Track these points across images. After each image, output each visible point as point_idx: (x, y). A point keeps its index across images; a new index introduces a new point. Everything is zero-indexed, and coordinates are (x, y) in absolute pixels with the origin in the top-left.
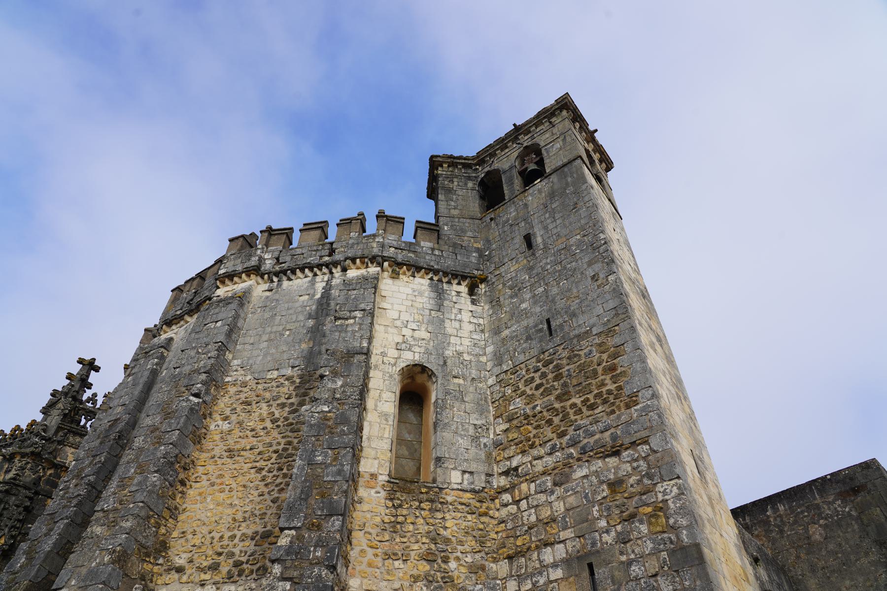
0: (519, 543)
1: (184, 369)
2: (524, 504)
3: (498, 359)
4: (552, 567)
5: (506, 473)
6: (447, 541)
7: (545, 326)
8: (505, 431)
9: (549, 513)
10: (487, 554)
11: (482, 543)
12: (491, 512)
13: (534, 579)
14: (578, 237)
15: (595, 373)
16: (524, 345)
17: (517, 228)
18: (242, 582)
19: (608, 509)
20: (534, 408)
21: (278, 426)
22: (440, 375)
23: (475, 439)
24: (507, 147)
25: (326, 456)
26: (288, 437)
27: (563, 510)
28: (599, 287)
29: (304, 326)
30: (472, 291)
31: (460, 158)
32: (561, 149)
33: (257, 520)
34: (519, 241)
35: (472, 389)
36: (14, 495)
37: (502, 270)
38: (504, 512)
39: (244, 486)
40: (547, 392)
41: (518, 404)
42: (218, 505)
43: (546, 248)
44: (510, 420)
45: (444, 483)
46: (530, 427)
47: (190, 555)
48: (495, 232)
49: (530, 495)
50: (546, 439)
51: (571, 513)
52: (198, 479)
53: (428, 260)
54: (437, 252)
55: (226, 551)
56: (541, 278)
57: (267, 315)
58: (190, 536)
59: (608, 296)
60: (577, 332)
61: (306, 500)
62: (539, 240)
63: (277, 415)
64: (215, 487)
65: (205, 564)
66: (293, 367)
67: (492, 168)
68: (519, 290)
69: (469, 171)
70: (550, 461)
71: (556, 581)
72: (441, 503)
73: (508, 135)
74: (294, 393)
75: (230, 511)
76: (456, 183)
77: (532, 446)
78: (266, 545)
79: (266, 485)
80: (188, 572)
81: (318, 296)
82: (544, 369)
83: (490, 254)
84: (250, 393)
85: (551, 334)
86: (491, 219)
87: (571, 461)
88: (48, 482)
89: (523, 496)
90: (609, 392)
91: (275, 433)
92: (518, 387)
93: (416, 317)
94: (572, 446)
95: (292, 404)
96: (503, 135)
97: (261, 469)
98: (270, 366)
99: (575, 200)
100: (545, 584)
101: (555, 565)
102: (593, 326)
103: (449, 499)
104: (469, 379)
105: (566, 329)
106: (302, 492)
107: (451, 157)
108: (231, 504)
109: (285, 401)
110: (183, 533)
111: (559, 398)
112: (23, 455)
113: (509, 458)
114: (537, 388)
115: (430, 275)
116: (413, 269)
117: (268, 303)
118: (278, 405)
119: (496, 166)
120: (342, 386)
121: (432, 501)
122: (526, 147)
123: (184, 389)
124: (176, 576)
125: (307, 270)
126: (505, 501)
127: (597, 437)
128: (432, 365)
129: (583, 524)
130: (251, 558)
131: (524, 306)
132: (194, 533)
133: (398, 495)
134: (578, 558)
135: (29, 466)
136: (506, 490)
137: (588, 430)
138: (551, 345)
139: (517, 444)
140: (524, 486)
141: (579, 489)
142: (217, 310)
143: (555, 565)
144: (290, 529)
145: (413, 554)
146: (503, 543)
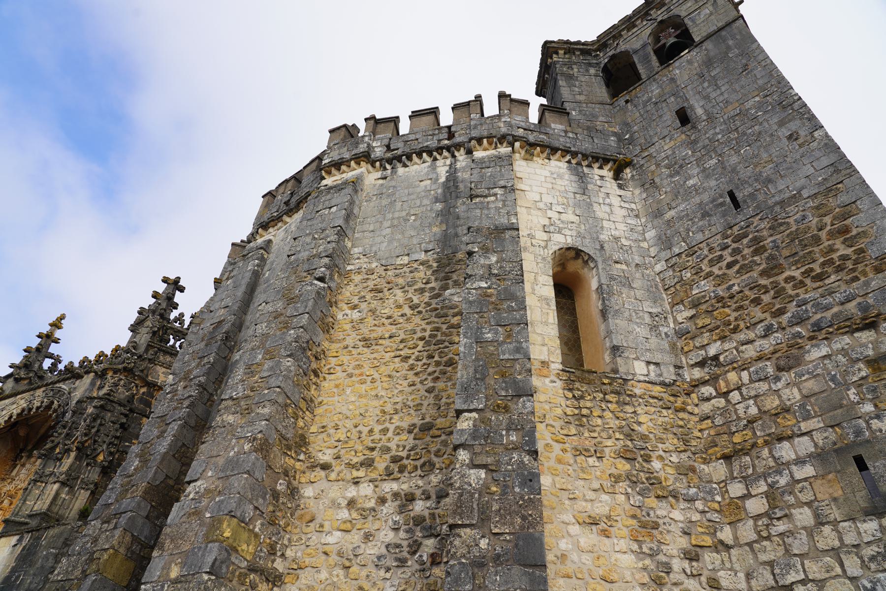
0: (737, 439)
1: (300, 256)
2: (735, 396)
3: (665, 242)
4: (796, 464)
5: (701, 364)
6: (644, 438)
7: (728, 199)
8: (691, 318)
9: (777, 402)
10: (694, 454)
11: (686, 442)
12: (689, 408)
13: (769, 480)
14: (757, 99)
15: (817, 240)
16: (701, 223)
17: (664, 105)
18: (405, 480)
19: (874, 390)
20: (730, 288)
21: (420, 312)
22: (600, 261)
23: (654, 328)
24: (634, 26)
25: (496, 333)
26: (434, 322)
27: (798, 397)
28: (800, 146)
29: (431, 209)
30: (617, 177)
31: (578, 43)
32: (711, 14)
33: (412, 412)
34: (669, 117)
35: (638, 275)
36: (109, 411)
37: (652, 150)
38: (706, 407)
39: (390, 376)
40: (745, 269)
41: (705, 286)
42: (360, 396)
43: (711, 118)
44: (695, 305)
45: (627, 373)
46: (727, 310)
47: (335, 451)
48: (633, 114)
49: (743, 385)
50: (754, 321)
51: (812, 400)
52: (332, 371)
53: (561, 142)
54: (571, 135)
55: (379, 445)
56: (711, 149)
57: (385, 202)
58: (332, 431)
59: (817, 154)
60: (777, 199)
61: (483, 379)
64: (354, 378)
65: (355, 460)
66: (426, 252)
67: (618, 50)
68: (681, 167)
69: (589, 58)
70: (767, 345)
71: (806, 479)
72: (629, 395)
73: (636, 12)
74: (433, 278)
75: (376, 403)
76: (576, 70)
77: (735, 330)
78: (428, 438)
79: (416, 374)
80: (337, 469)
81: (443, 179)
82: (734, 245)
83: (631, 136)
84: (378, 280)
86: (627, 102)
87: (800, 341)
88: (141, 400)
89: (732, 387)
90: (844, 258)
91: (417, 320)
92: (701, 269)
93: (560, 199)
94: (797, 324)
95: (433, 289)
96: (629, 12)
97: (406, 358)
99: (744, 61)
100: (787, 484)
101: (800, 461)
102: (803, 188)
103: (638, 391)
104: (633, 265)
105: (761, 197)
106: (476, 371)
107: (568, 42)
108: (377, 396)
109: (423, 286)
110: (323, 427)
111: (763, 274)
112: (116, 371)
113: (703, 347)
114: (729, 266)
115: (568, 157)
116: (548, 151)
117: (384, 190)
118: (415, 290)
119: (623, 47)
120: (497, 262)
121: (618, 393)
122: (661, 22)
123: (305, 274)
124: (323, 473)
125: (424, 155)
126: (706, 395)
127: (835, 309)
128: (588, 247)
129: (836, 411)
130: (412, 453)
131: (691, 182)
132: (337, 428)
133: (577, 385)
134: (836, 451)
135: (122, 383)
136: (705, 383)
137: (819, 304)
138: (740, 217)
139: (711, 331)
140: (732, 376)
141: (819, 371)
142: (329, 197)
143: (800, 461)
144: (470, 411)
145: (607, 450)
146: (713, 441)
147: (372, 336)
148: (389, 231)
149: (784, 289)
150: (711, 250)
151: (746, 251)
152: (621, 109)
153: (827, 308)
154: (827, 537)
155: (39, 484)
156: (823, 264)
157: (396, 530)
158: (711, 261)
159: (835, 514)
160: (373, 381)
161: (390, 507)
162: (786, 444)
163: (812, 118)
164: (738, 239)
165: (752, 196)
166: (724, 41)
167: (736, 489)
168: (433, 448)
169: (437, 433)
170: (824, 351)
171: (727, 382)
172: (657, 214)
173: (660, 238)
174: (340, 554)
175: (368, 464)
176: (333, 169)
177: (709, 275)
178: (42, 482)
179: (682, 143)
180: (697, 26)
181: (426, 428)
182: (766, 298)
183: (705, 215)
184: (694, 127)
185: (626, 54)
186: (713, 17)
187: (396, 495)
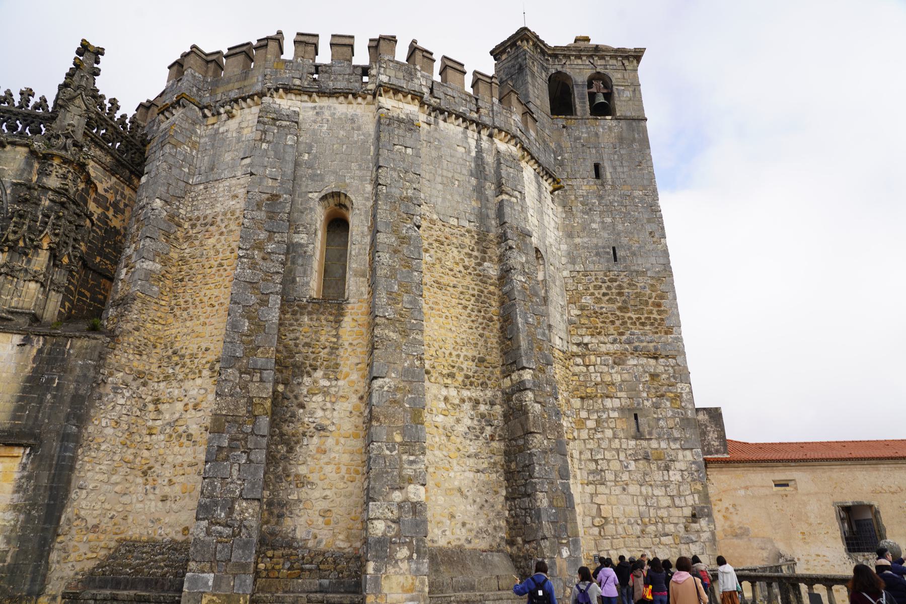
0: (589, 390)
2: (591, 368)
5: (578, 345)
15: (647, 303)
19: (649, 388)
20: (602, 308)
21: (470, 274)
28: (654, 242)
31: (542, 42)
32: (630, 100)
38: (577, 369)
41: (587, 300)
42: (440, 327)
43: (613, 186)
44: (582, 309)
56: (609, 209)
60: (636, 268)
62: (608, 173)
63: (467, 263)
65: (444, 372)
67: (564, 70)
70: (612, 348)
75: (450, 334)
77: (599, 333)
78: (483, 368)
79: (473, 321)
81: (473, 154)
82: (609, 283)
83: (562, 160)
85: (615, 260)
86: (564, 127)
90: (655, 319)
91: (468, 278)
95: (476, 257)
97: (465, 307)
98: (450, 212)
101: (613, 409)
105: (628, 262)
107: (537, 37)
111: (620, 308)
112: (65, 161)
114: (604, 295)
116: (529, 157)
117: (432, 140)
119: (567, 70)
122: (599, 73)
123: (405, 216)
127: (645, 344)
129: (633, 392)
131: (594, 226)
136: (579, 356)
140: (593, 358)
142: (401, 132)
143: (613, 409)
147: (442, 281)
148: (440, 187)
149: (626, 322)
150: (597, 279)
151: (614, 290)
152: (558, 129)
153: (642, 341)
154: (616, 444)
155: (9, 277)
156: (646, 318)
157: (472, 419)
158: (595, 286)
159: (621, 435)
160: (447, 317)
161: (467, 406)
162: (609, 400)
163: (663, 228)
164: (611, 280)
165: (624, 257)
166: (633, 131)
167: (583, 414)
168: (487, 374)
169: (488, 365)
170: (635, 362)
171: (590, 360)
172: (570, 235)
173: (569, 254)
174: (444, 428)
175: (451, 375)
176: (391, 92)
177: (592, 294)
178: (13, 277)
179: (594, 193)
180: (620, 101)
181: (482, 360)
182: (618, 323)
183: (597, 254)
184: (602, 185)
185: (569, 77)
186: (631, 103)
187: (470, 399)
